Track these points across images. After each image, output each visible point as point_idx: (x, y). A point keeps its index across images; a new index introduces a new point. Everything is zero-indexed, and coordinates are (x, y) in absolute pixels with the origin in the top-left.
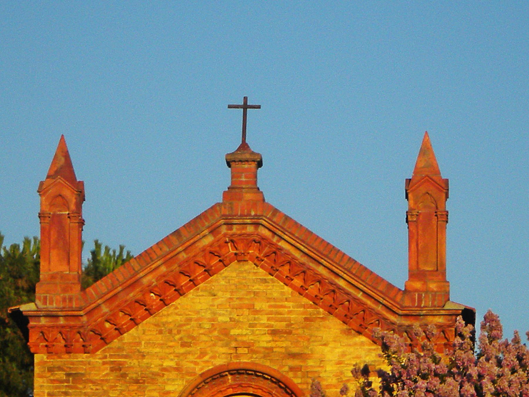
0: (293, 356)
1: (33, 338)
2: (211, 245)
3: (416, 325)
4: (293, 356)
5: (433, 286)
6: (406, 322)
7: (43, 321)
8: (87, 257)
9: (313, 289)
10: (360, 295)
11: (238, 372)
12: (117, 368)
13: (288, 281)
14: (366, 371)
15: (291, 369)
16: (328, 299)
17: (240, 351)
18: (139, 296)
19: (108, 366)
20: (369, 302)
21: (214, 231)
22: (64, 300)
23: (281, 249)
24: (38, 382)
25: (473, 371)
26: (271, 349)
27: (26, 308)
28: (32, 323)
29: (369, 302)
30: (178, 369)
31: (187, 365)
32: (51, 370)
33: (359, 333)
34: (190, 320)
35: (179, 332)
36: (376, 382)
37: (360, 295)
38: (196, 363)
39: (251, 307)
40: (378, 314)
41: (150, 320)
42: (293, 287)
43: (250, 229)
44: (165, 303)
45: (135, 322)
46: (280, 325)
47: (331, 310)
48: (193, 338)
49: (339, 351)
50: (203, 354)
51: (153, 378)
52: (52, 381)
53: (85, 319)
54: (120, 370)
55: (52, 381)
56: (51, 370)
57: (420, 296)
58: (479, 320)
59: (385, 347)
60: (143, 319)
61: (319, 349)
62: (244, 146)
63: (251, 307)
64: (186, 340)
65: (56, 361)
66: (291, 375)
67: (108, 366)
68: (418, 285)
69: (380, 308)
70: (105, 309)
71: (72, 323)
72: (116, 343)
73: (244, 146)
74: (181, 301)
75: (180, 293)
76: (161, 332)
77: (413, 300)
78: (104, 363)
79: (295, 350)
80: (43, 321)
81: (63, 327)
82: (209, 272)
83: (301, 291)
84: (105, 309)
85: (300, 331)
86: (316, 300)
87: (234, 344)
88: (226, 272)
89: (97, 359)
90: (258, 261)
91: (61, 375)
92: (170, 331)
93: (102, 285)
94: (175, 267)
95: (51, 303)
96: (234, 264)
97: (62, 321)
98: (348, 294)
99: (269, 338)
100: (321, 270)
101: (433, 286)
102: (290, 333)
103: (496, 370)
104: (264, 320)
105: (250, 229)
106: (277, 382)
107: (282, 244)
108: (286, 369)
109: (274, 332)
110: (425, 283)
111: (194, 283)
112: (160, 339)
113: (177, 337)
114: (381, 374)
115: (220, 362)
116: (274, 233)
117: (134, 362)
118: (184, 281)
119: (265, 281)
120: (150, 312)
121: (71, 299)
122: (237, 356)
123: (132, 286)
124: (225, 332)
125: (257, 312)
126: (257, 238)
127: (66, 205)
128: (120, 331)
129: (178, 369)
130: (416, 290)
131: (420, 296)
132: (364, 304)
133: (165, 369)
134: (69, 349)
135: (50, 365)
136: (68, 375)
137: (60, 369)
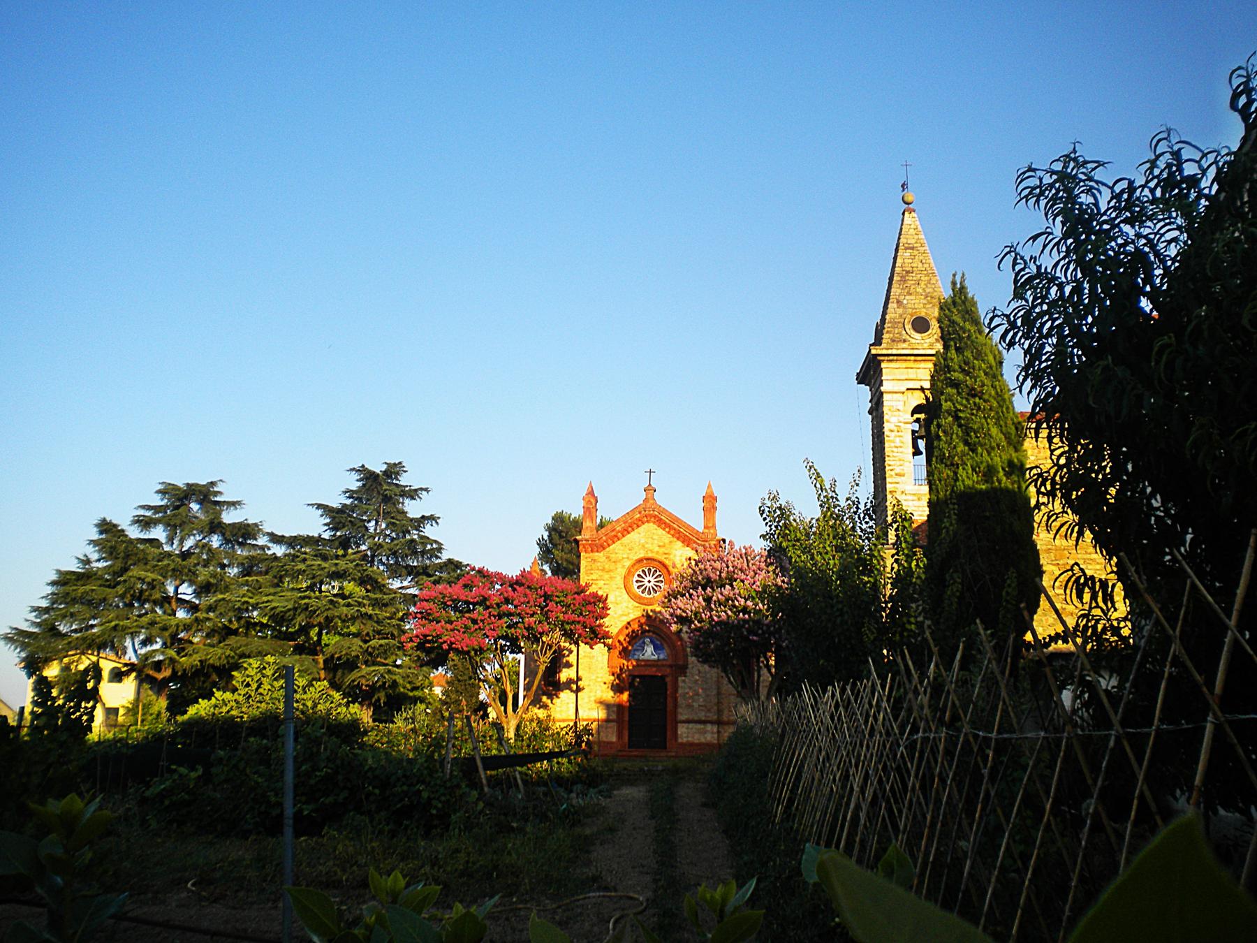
0: (665, 554)
1: (581, 547)
3: (707, 544)
4: (665, 554)
5: (712, 531)
6: (703, 543)
7: (584, 542)
8: (598, 521)
9: (672, 532)
11: (648, 559)
12: (608, 557)
13: (664, 529)
14: (690, 559)
16: (677, 535)
21: (640, 513)
25: (725, 559)
27: (578, 538)
30: (628, 558)
31: (631, 556)
36: (693, 563)
39: (652, 538)
41: (619, 542)
44: (624, 536)
45: (614, 542)
46: (661, 544)
47: (678, 539)
49: (681, 552)
51: (620, 561)
58: (727, 542)
59: (697, 551)
61: (674, 552)
62: (650, 485)
63: (652, 538)
65: (587, 555)
68: (706, 531)
70: (604, 538)
72: (608, 549)
73: (650, 485)
74: (629, 535)
75: (629, 533)
79: (666, 552)
80: (584, 542)
82: (638, 526)
83: (669, 533)
84: (604, 538)
86: (673, 536)
88: (644, 526)
89: (602, 554)
90: (654, 523)
91: (590, 560)
93: (603, 530)
94: (627, 525)
96: (646, 524)
100: (675, 526)
101: (712, 531)
103: (733, 559)
104: (656, 542)
106: (660, 562)
109: (659, 546)
111: (633, 530)
112: (622, 548)
114: (695, 560)
115: (642, 556)
117: (613, 556)
118: (630, 529)
120: (619, 539)
123: (613, 531)
124: (643, 546)
127: (591, 504)
128: (609, 545)
129: (628, 558)
133: (623, 558)
134: (592, 551)
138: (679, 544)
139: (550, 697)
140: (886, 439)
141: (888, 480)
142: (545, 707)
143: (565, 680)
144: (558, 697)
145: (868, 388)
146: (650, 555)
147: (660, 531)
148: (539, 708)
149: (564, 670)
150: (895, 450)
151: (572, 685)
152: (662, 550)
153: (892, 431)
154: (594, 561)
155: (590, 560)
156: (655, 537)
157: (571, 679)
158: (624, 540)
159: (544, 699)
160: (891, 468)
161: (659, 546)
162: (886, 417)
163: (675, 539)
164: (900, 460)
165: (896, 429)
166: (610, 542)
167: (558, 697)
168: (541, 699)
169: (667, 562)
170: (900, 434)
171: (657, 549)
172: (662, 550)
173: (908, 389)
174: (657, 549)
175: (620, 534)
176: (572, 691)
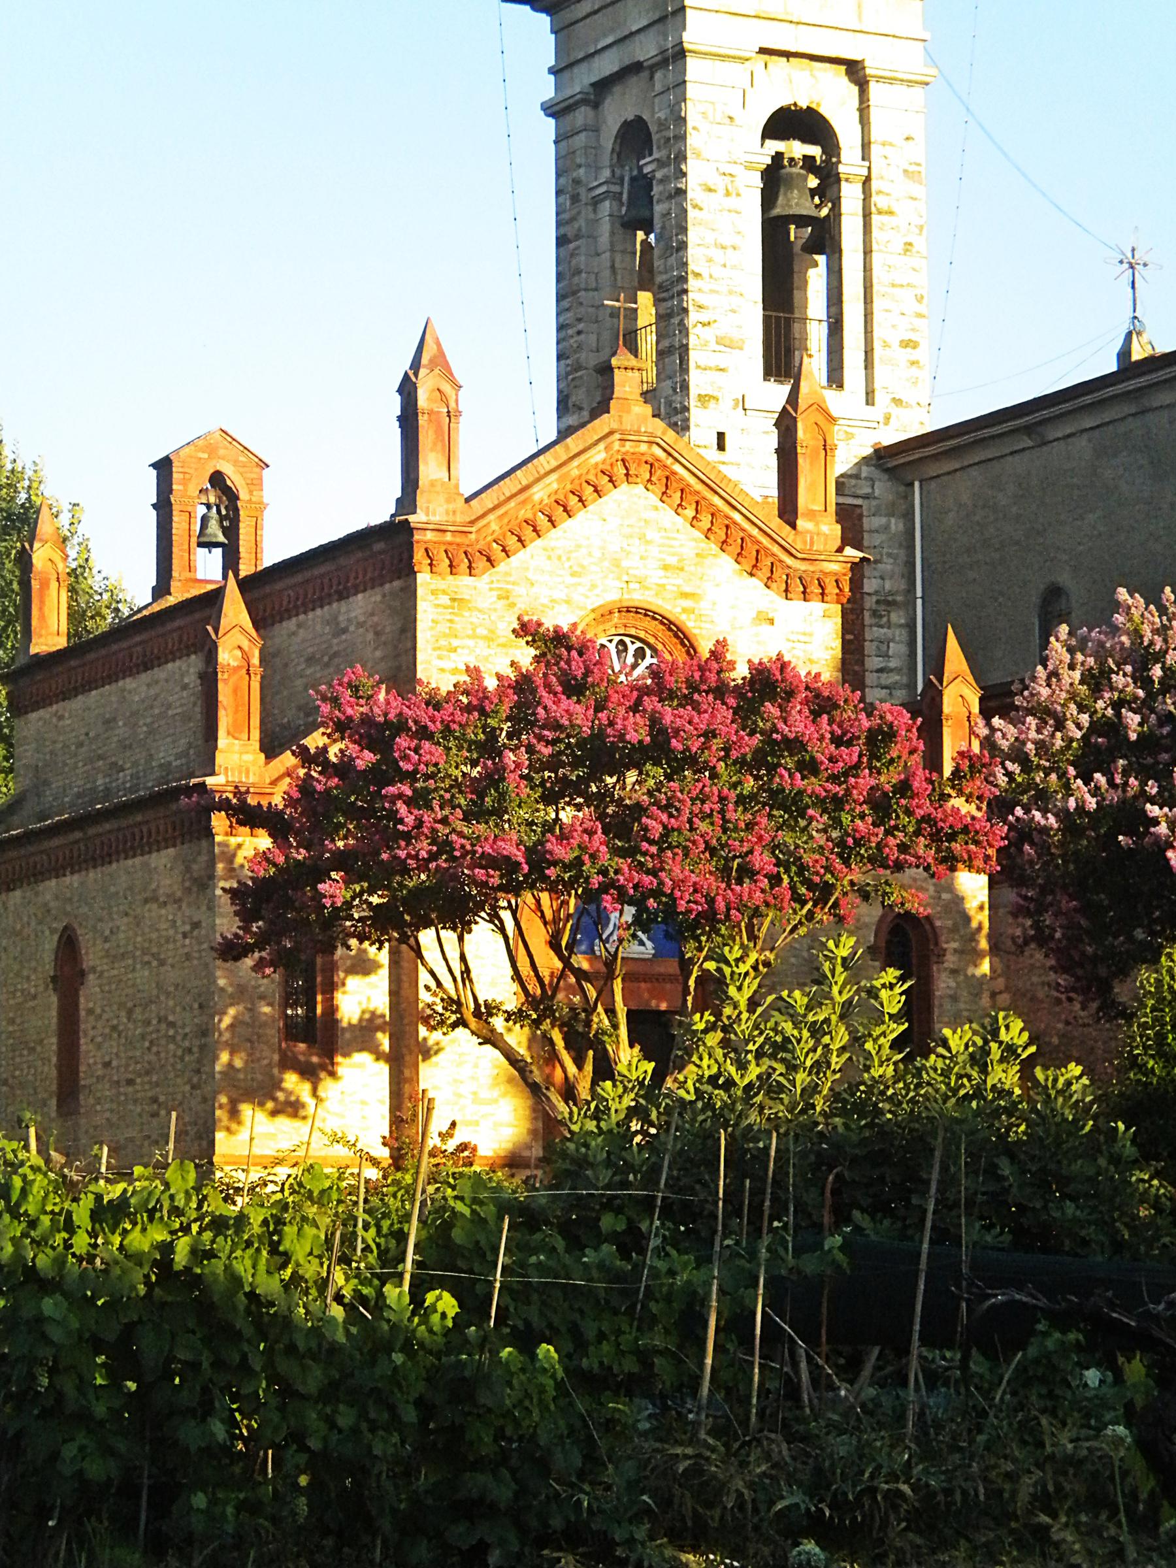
0: (685, 595)
2: (604, 462)
4: (685, 595)
7: (429, 535)
10: (755, 532)
12: (505, 596)
15: (684, 610)
17: (632, 586)
18: (529, 515)
19: (495, 593)
20: (765, 541)
22: (447, 513)
23: (674, 473)
24: (421, 606)
26: (663, 586)
28: (417, 537)
29: (765, 541)
30: (568, 602)
32: (434, 592)
33: (751, 574)
34: (578, 546)
35: (568, 559)
37: (755, 532)
38: (587, 597)
39: (642, 537)
40: (773, 555)
42: (685, 518)
43: (643, 448)
46: (672, 560)
47: (724, 545)
48: (583, 567)
50: (593, 586)
52: (437, 606)
53: (473, 536)
54: (507, 598)
55: (437, 606)
56: (434, 592)
57: (812, 539)
60: (532, 541)
63: (642, 537)
64: (575, 569)
66: (683, 617)
67: (495, 593)
69: (776, 549)
71: (458, 540)
72: (502, 567)
76: (549, 558)
77: (805, 542)
78: (491, 589)
79: (688, 590)
80: (429, 535)
81: (450, 544)
85: (692, 568)
87: (625, 578)
92: (559, 558)
95: (434, 514)
97: (448, 537)
98: (743, 530)
99: (662, 573)
100: (716, 500)
102: (682, 569)
105: (643, 448)
107: (677, 468)
108: (679, 610)
109: (666, 567)
110: (817, 524)
113: (567, 565)
116: (670, 454)
119: (657, 509)
121: (454, 512)
122: (629, 592)
124: (616, 563)
125: (648, 542)
126: (650, 460)
130: (808, 532)
131: (812, 539)
132: (759, 542)
133: (553, 601)
135: (433, 587)
136: (453, 600)
137: (444, 592)
138: (726, 562)
139: (310, 1073)
140: (692, 214)
141: (694, 356)
142: (293, 1108)
143: (355, 1021)
144: (332, 1074)
145: (544, 20)
146: (638, 597)
147: (666, 514)
148: (274, 1113)
149: (354, 983)
150: (718, 254)
151: (379, 1035)
152: (675, 581)
153: (710, 190)
154: (457, 601)
155: (444, 600)
156: (652, 534)
157: (373, 1013)
158: (553, 537)
159: (291, 1080)
160: (704, 316)
161: (666, 567)
162: (693, 141)
163: (714, 548)
164: (730, 292)
165: (720, 183)
166: (512, 541)
167: (332, 1074)
168: (281, 1080)
169: (690, 624)
170: (732, 202)
171: (656, 576)
172: (675, 581)
173: (763, 51)
174: (656, 576)
175: (542, 520)
176: (379, 1056)
